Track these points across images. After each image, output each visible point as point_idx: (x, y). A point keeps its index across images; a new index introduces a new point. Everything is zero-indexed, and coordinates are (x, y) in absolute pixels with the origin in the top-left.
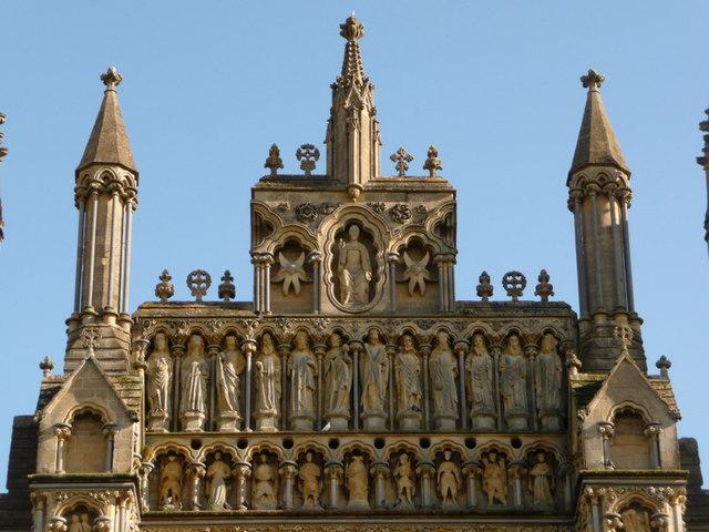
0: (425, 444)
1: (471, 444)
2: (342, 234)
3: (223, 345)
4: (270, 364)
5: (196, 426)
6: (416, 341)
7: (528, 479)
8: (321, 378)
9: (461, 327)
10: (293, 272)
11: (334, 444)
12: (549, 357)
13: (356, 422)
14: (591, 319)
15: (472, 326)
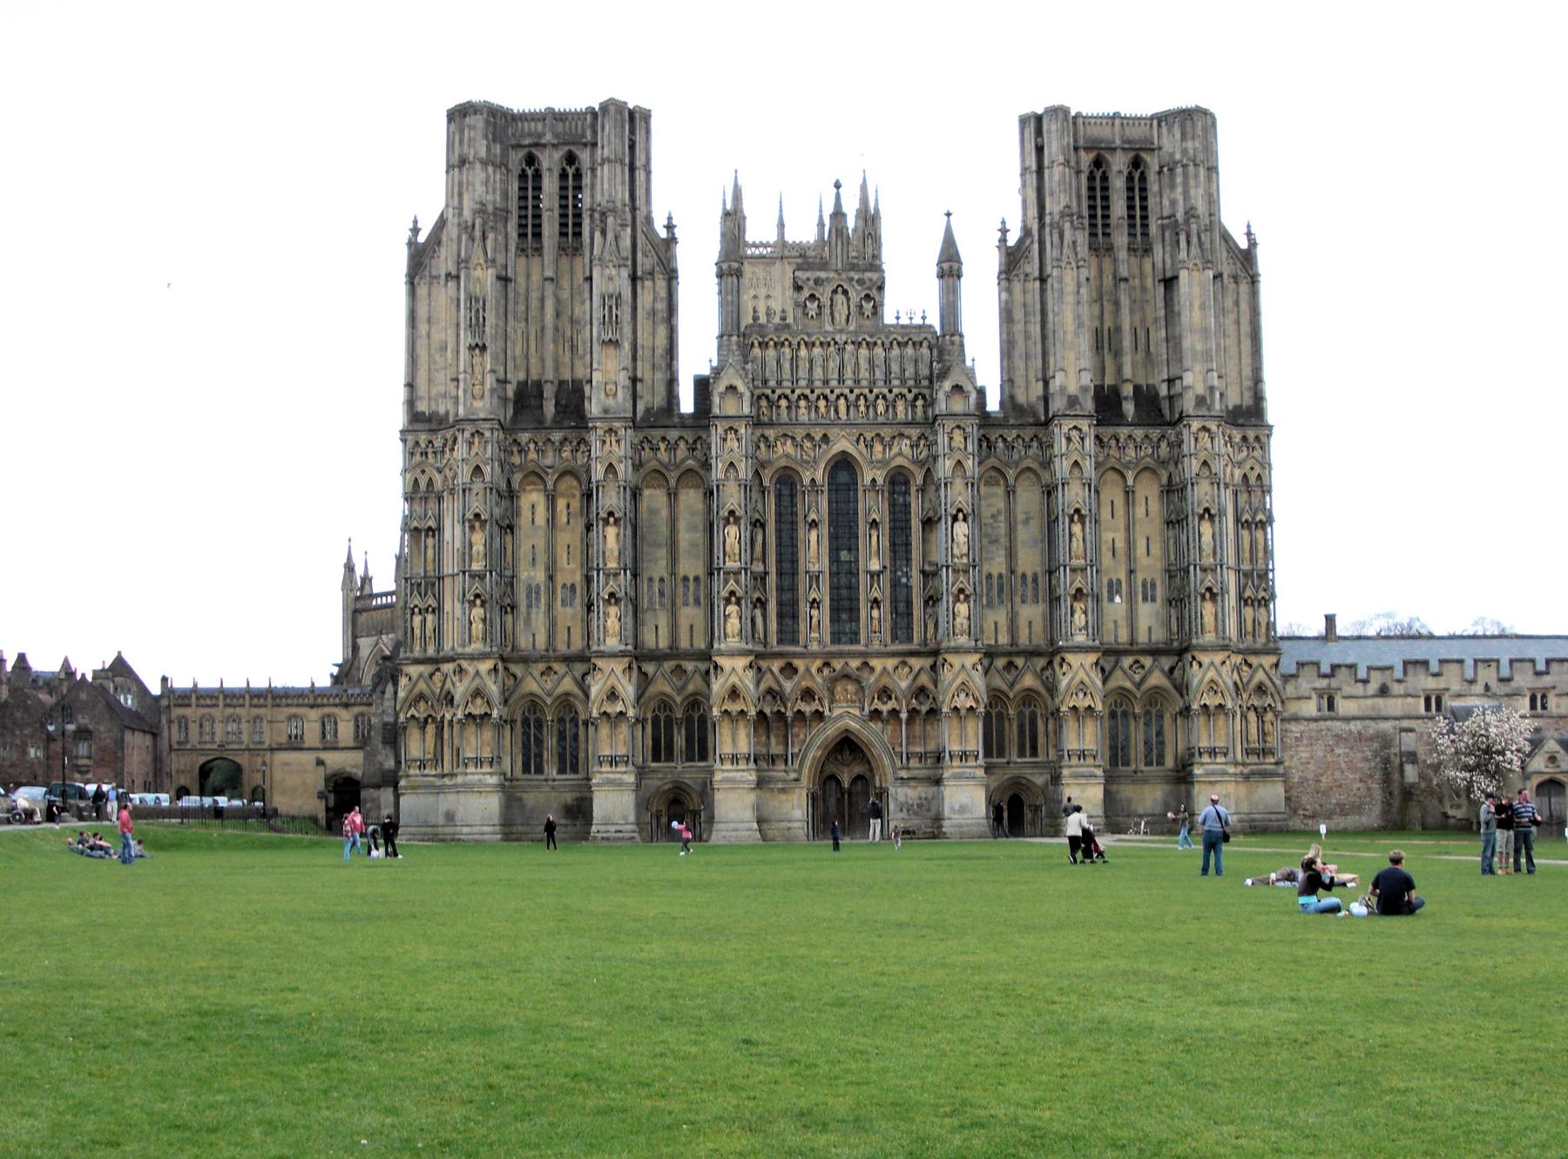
0: (871, 391)
1: (890, 391)
2: (835, 292)
3: (783, 344)
4: (803, 352)
5: (772, 383)
6: (868, 344)
7: (914, 407)
8: (826, 360)
9: (887, 337)
10: (812, 307)
11: (832, 392)
12: (925, 351)
13: (841, 380)
14: (944, 336)
15: (891, 338)
